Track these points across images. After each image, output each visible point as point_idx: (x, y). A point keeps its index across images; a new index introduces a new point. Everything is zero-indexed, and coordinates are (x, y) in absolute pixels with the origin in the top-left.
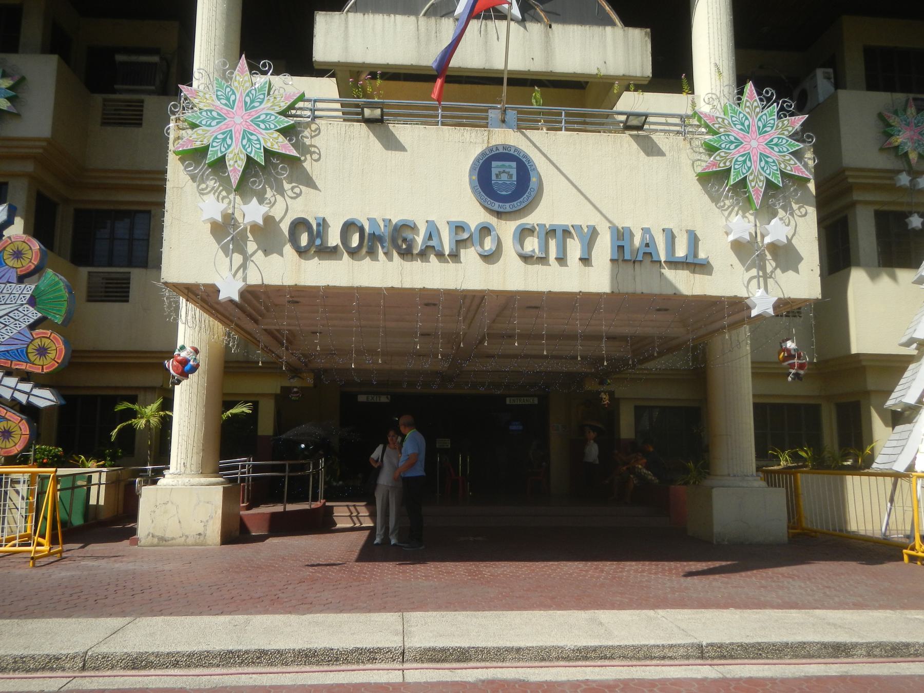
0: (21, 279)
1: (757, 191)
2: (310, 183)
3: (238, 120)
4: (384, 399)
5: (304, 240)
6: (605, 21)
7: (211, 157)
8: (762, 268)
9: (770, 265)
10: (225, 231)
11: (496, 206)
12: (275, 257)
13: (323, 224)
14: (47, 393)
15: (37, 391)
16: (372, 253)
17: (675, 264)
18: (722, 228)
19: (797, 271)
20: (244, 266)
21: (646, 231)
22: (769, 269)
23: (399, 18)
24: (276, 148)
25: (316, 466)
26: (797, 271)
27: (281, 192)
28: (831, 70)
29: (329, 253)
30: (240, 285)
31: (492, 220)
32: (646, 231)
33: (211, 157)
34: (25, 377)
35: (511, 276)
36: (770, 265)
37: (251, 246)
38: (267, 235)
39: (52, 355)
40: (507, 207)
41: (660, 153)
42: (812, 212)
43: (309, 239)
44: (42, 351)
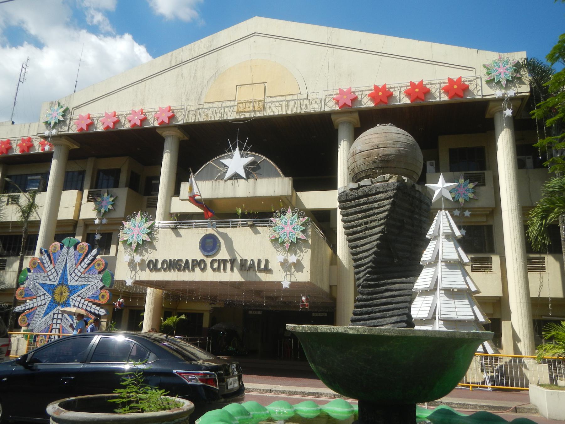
0: (99, 273)
1: (287, 245)
2: (155, 248)
3: (136, 231)
4: (259, 313)
5: (151, 266)
6: (278, 175)
7: (128, 243)
8: (290, 271)
9: (293, 270)
10: (132, 265)
11: (206, 254)
12: (144, 271)
13: (157, 261)
14: (103, 310)
15: (101, 310)
16: (170, 270)
17: (260, 270)
18: (276, 258)
19: (302, 272)
20: (135, 274)
21: (252, 260)
22: (292, 272)
23: (207, 181)
24: (145, 239)
25: (209, 339)
26: (302, 272)
27: (147, 252)
28: (434, 162)
29: (158, 270)
30: (132, 281)
31: (205, 258)
32: (252, 260)
33: (128, 243)
34: (98, 305)
35: (210, 276)
36: (293, 270)
37: (138, 268)
38: (142, 265)
39: (105, 298)
40: (209, 254)
41: (259, 233)
42: (309, 250)
43: (153, 266)
44: (103, 297)
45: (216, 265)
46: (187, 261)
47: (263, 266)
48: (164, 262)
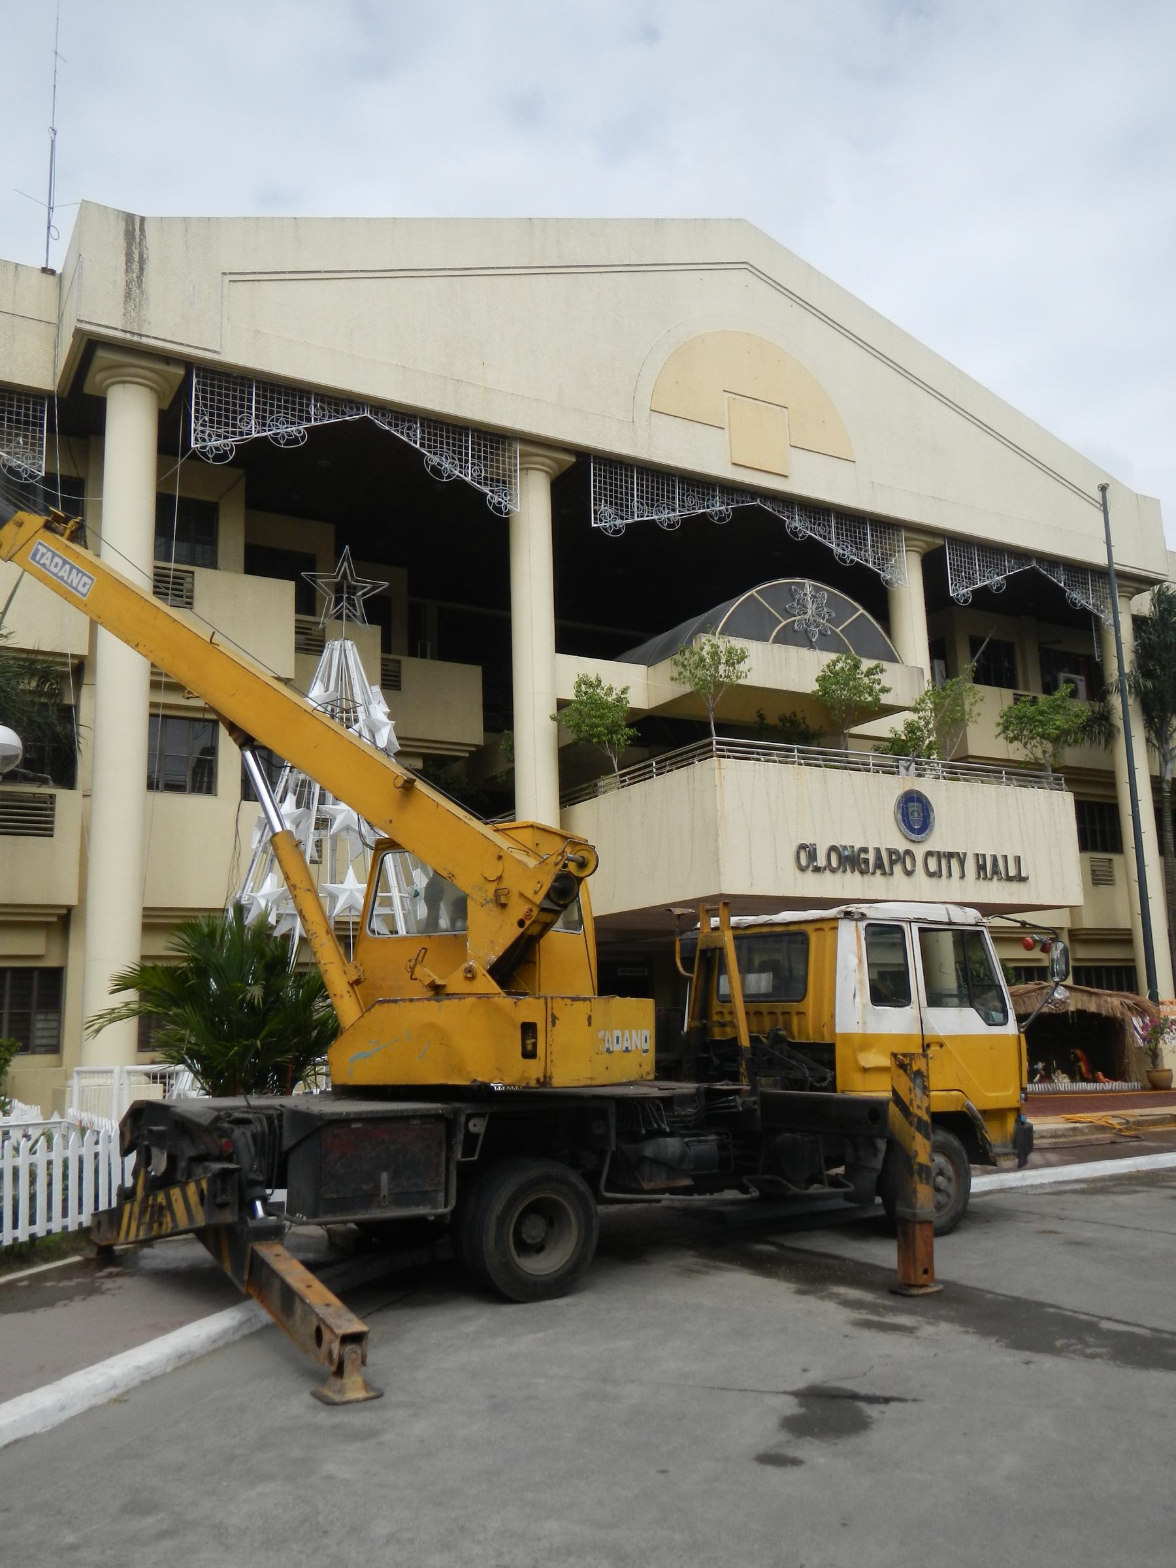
5: (804, 862)
11: (913, 836)
45: (933, 867)
46: (878, 850)
47: (1012, 873)
48: (833, 848)
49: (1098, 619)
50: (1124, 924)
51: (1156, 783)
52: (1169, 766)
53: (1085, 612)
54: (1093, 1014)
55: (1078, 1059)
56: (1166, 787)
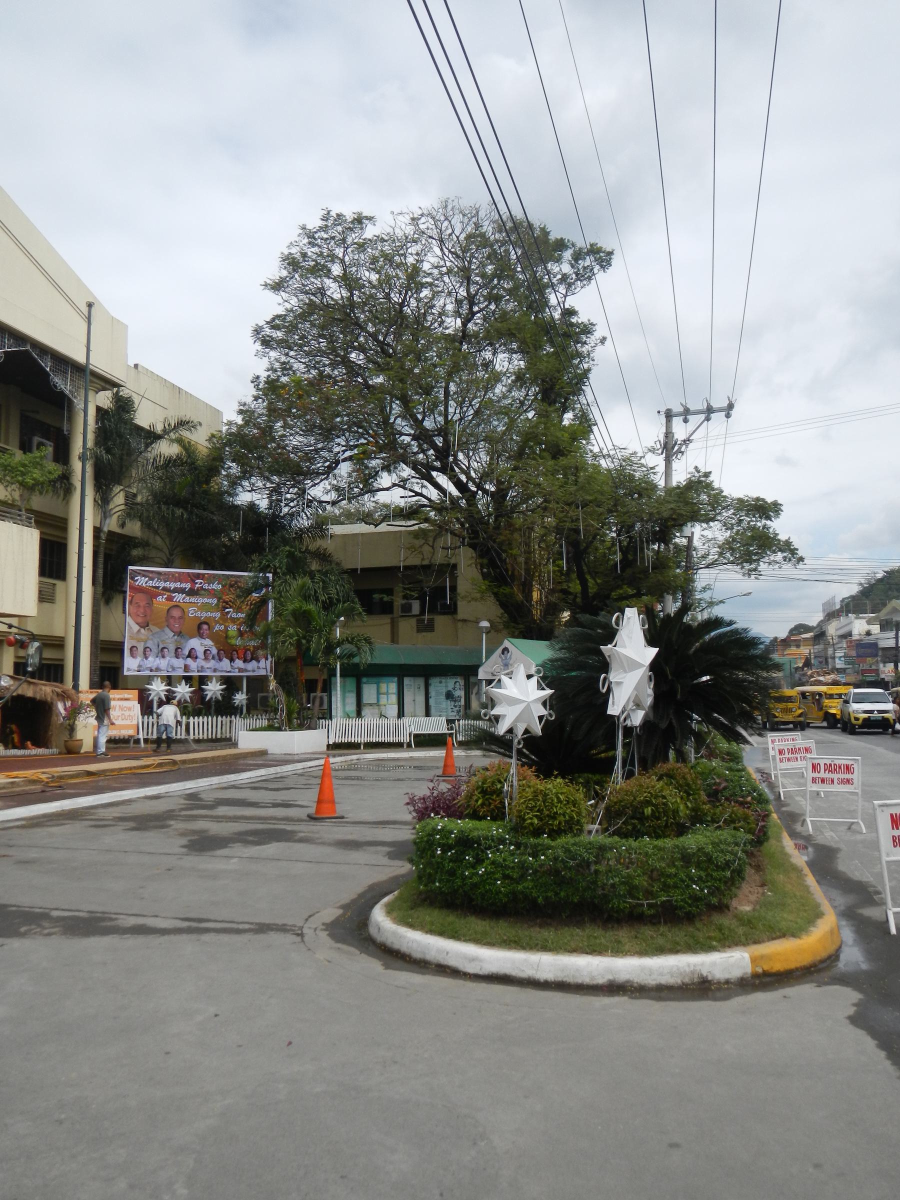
49: (70, 402)
50: (58, 632)
51: (97, 531)
52: (108, 521)
53: (62, 393)
54: (30, 698)
55: (12, 732)
56: (103, 536)
